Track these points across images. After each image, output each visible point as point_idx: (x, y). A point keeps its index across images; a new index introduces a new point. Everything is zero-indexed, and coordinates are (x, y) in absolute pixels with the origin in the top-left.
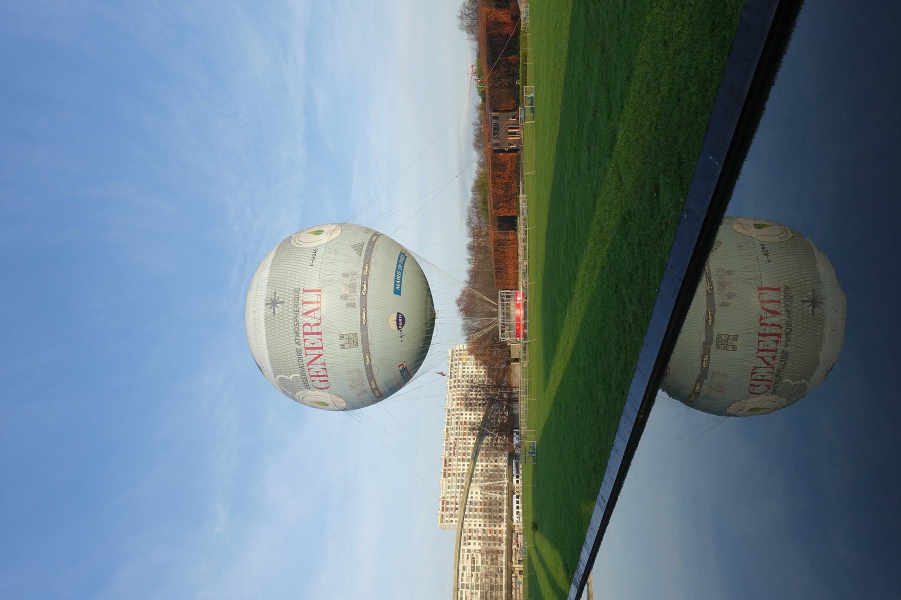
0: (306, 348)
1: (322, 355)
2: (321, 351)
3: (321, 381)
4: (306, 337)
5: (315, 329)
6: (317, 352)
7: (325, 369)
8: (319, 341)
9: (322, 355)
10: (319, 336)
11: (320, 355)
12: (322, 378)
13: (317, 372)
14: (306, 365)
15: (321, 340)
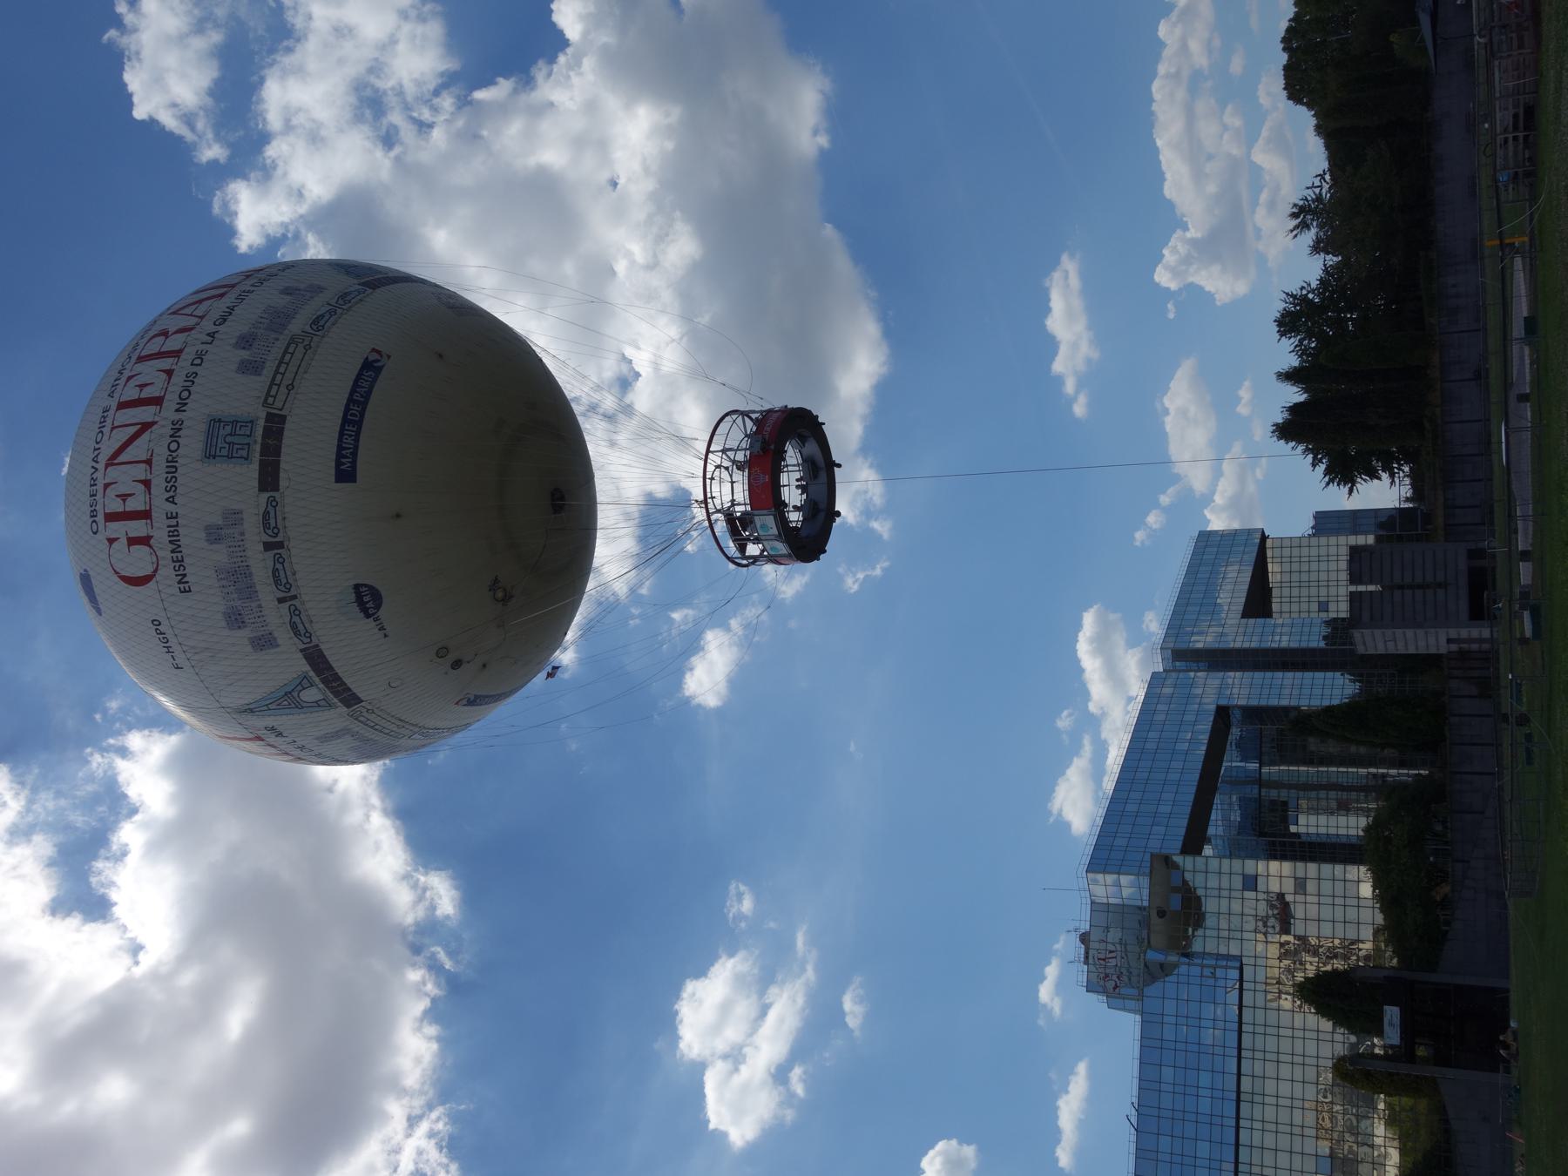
0: (123, 405)
1: (153, 423)
2: (152, 409)
3: (133, 541)
4: (139, 368)
5: (174, 343)
6: (145, 414)
7: (147, 484)
8: (164, 376)
9: (153, 423)
10: (166, 363)
11: (146, 426)
12: (138, 528)
13: (124, 497)
14: (101, 466)
15: (169, 373)
